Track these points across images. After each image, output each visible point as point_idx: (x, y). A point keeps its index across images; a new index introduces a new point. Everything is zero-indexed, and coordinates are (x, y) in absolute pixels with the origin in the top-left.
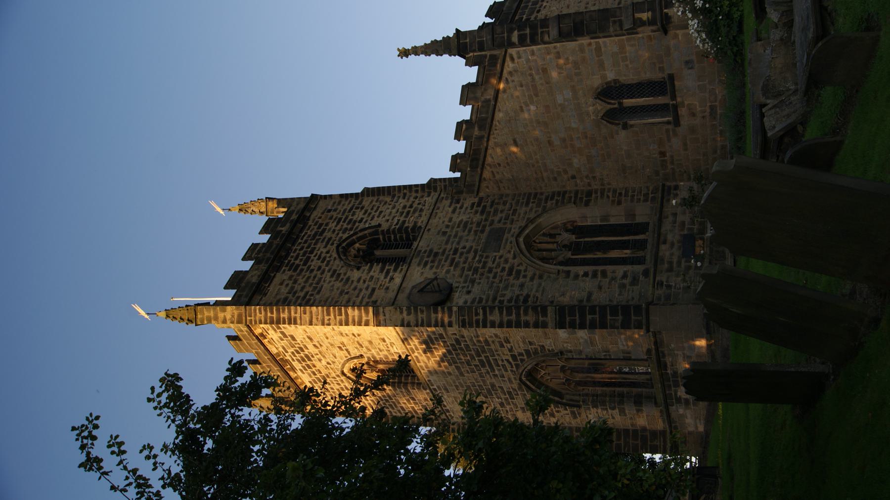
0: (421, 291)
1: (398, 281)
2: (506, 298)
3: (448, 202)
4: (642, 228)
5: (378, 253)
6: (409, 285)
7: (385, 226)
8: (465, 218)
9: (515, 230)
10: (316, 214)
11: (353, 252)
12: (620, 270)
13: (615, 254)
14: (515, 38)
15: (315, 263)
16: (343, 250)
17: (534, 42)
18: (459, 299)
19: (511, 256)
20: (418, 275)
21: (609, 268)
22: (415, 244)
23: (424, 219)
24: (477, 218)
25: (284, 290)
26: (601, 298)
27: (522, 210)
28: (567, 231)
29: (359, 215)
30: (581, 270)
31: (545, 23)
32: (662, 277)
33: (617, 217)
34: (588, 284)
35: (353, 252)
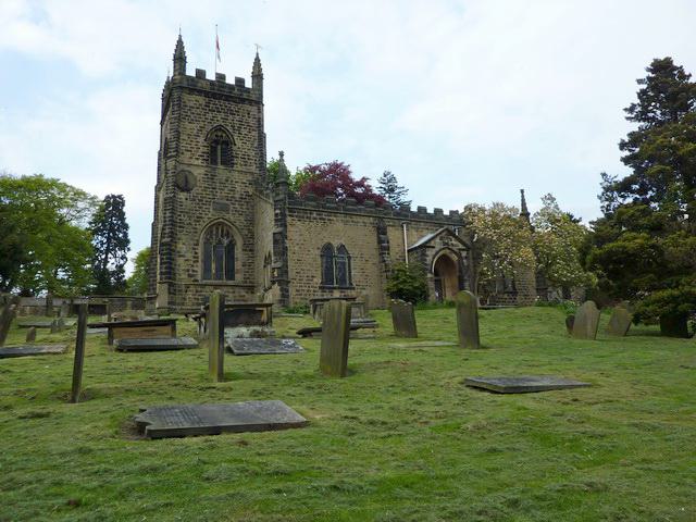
0: (186, 177)
1: (196, 162)
2: (182, 217)
3: (250, 178)
4: (231, 276)
5: (219, 147)
6: (191, 169)
7: (234, 148)
8: (238, 189)
9: (227, 217)
10: (247, 107)
11: (219, 134)
12: (199, 268)
13: (213, 266)
14: (278, 211)
15: (210, 115)
16: (219, 128)
17: (276, 220)
18: (182, 196)
19: (210, 216)
20: (199, 172)
21: (200, 264)
22: (222, 167)
23: (240, 168)
24: (237, 196)
25: (192, 104)
26: (181, 261)
27: (242, 218)
28: (231, 242)
29: (244, 132)
30: (200, 250)
31: (285, 226)
32: (192, 288)
33: (238, 265)
34: (189, 256)
35: (219, 134)
